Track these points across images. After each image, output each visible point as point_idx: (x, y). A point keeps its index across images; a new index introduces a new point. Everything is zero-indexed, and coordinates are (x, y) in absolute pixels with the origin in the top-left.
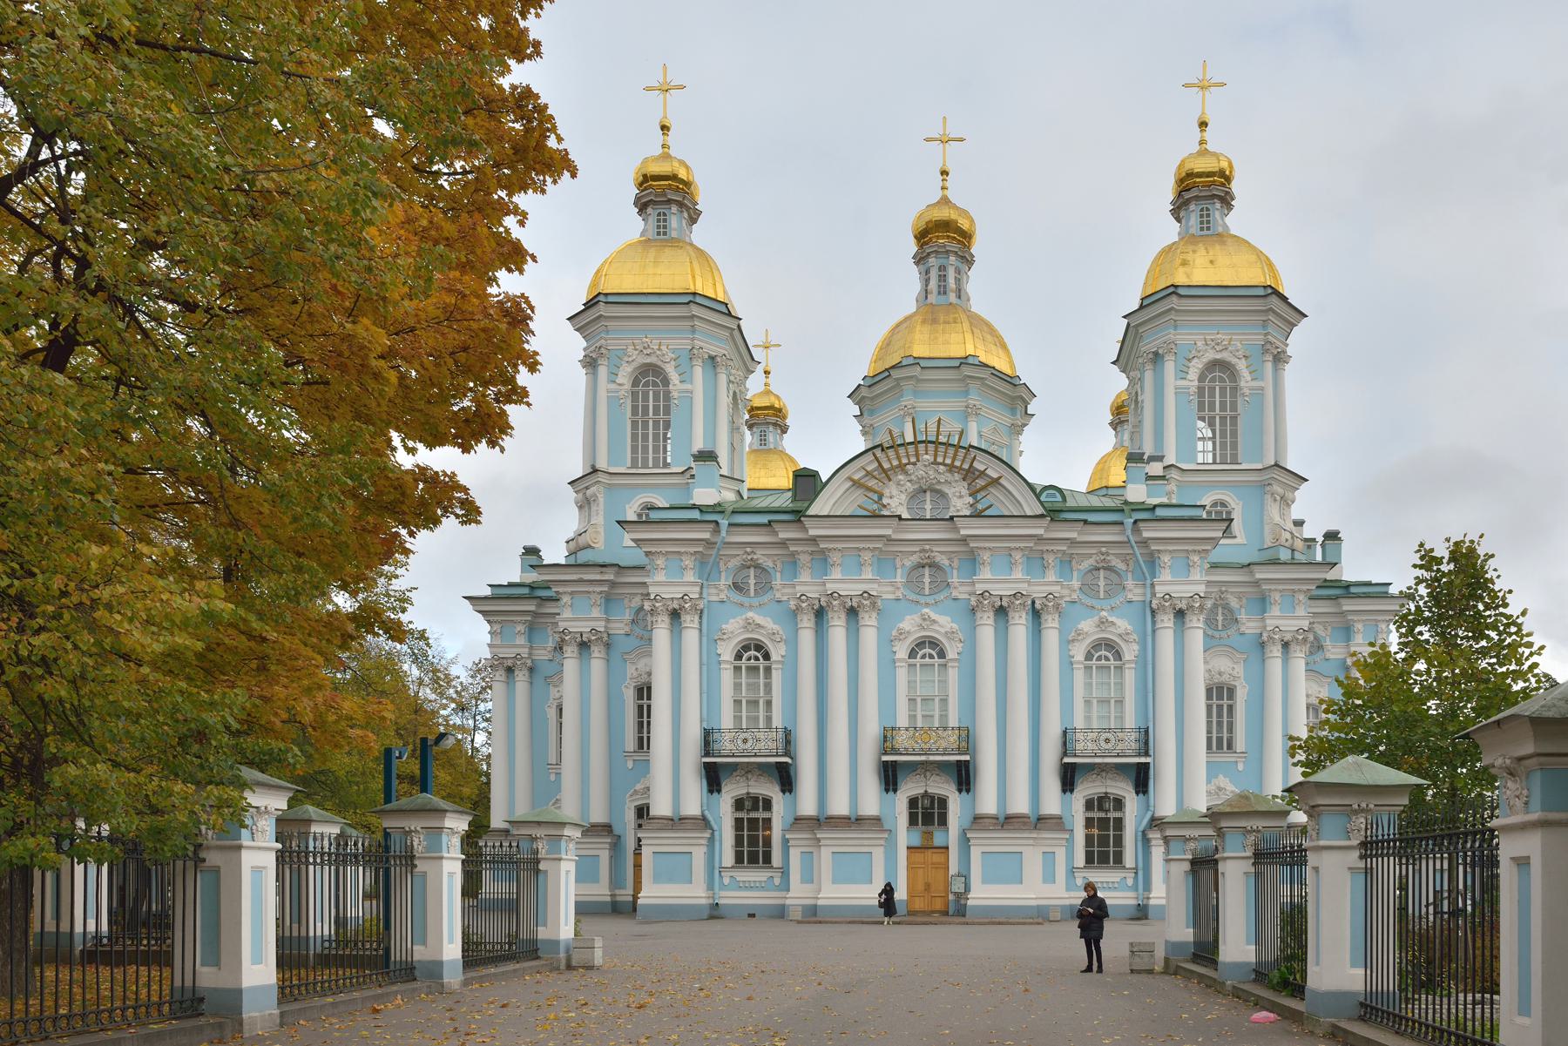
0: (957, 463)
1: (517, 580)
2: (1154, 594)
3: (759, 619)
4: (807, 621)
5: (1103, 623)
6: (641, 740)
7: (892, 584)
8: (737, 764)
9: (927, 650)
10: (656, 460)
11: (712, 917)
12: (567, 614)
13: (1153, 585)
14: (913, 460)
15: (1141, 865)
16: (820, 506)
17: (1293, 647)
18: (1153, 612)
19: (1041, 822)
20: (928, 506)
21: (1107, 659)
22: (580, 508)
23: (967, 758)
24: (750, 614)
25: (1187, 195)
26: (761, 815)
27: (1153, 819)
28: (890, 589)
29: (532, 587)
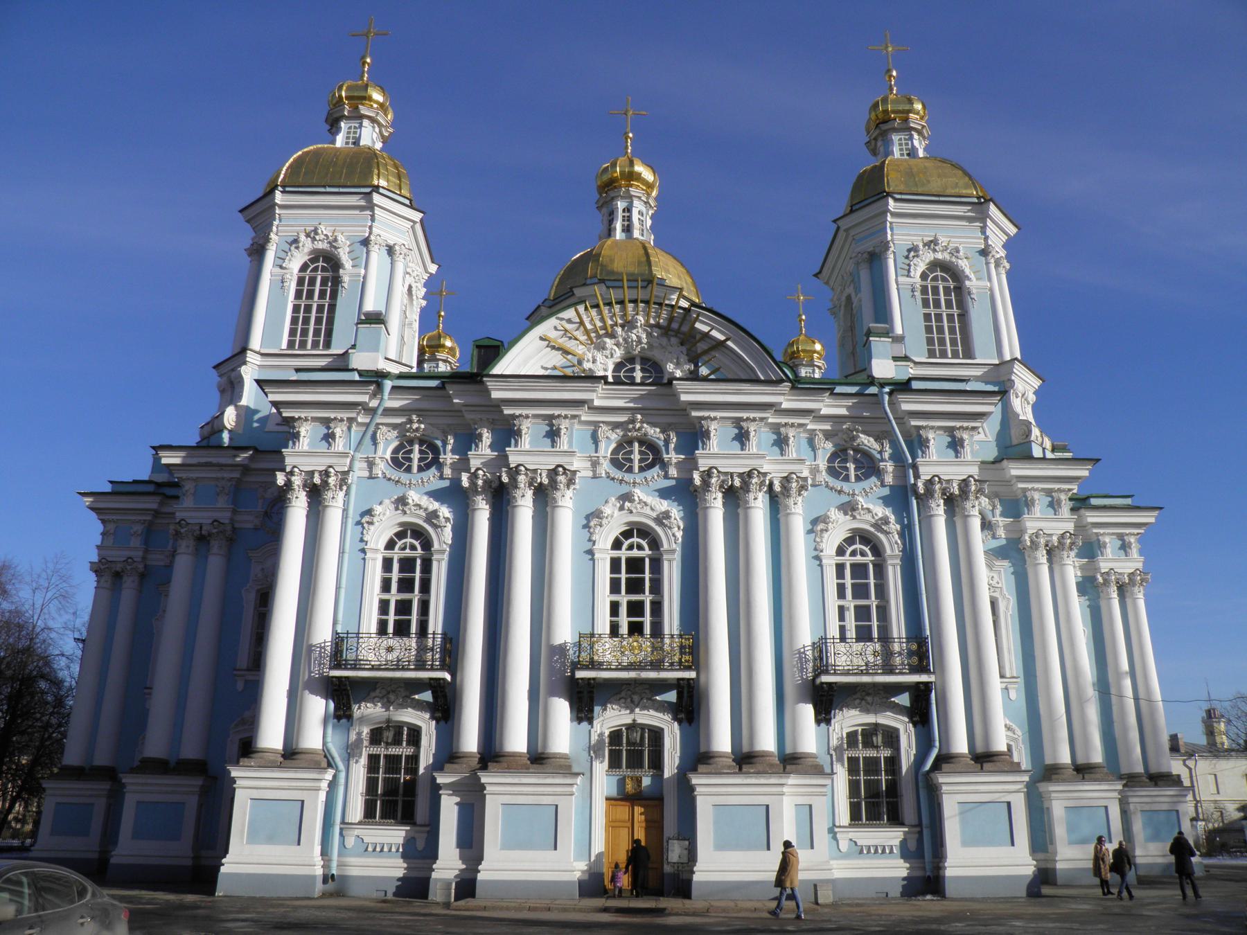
1: (146, 478)
9: (635, 540)
10: (315, 345)
12: (188, 502)
13: (915, 467)
15: (925, 821)
22: (222, 391)
23: (693, 675)
25: (884, 127)
29: (159, 485)
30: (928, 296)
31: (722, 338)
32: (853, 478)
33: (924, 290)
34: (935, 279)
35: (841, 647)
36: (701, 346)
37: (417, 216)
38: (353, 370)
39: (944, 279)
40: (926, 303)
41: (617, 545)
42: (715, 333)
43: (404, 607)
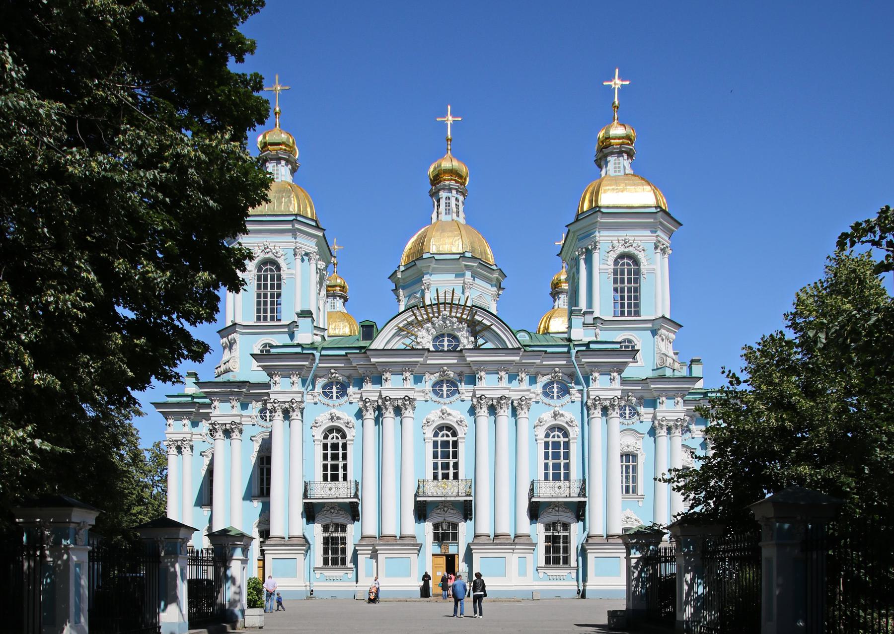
0: (464, 317)
2: (588, 397)
3: (338, 413)
5: (555, 415)
6: (262, 489)
8: (324, 503)
11: (308, 598)
14: (436, 315)
16: (378, 343)
17: (673, 431)
18: (588, 409)
19: (518, 541)
20: (446, 343)
21: (558, 437)
24: (333, 411)
26: (339, 535)
27: (589, 537)
30: (617, 276)
31: (488, 324)
32: (555, 397)
33: (615, 272)
34: (623, 264)
35: (543, 484)
37: (321, 234)
38: (299, 345)
39: (629, 265)
40: (615, 281)
41: (436, 435)
43: (335, 468)
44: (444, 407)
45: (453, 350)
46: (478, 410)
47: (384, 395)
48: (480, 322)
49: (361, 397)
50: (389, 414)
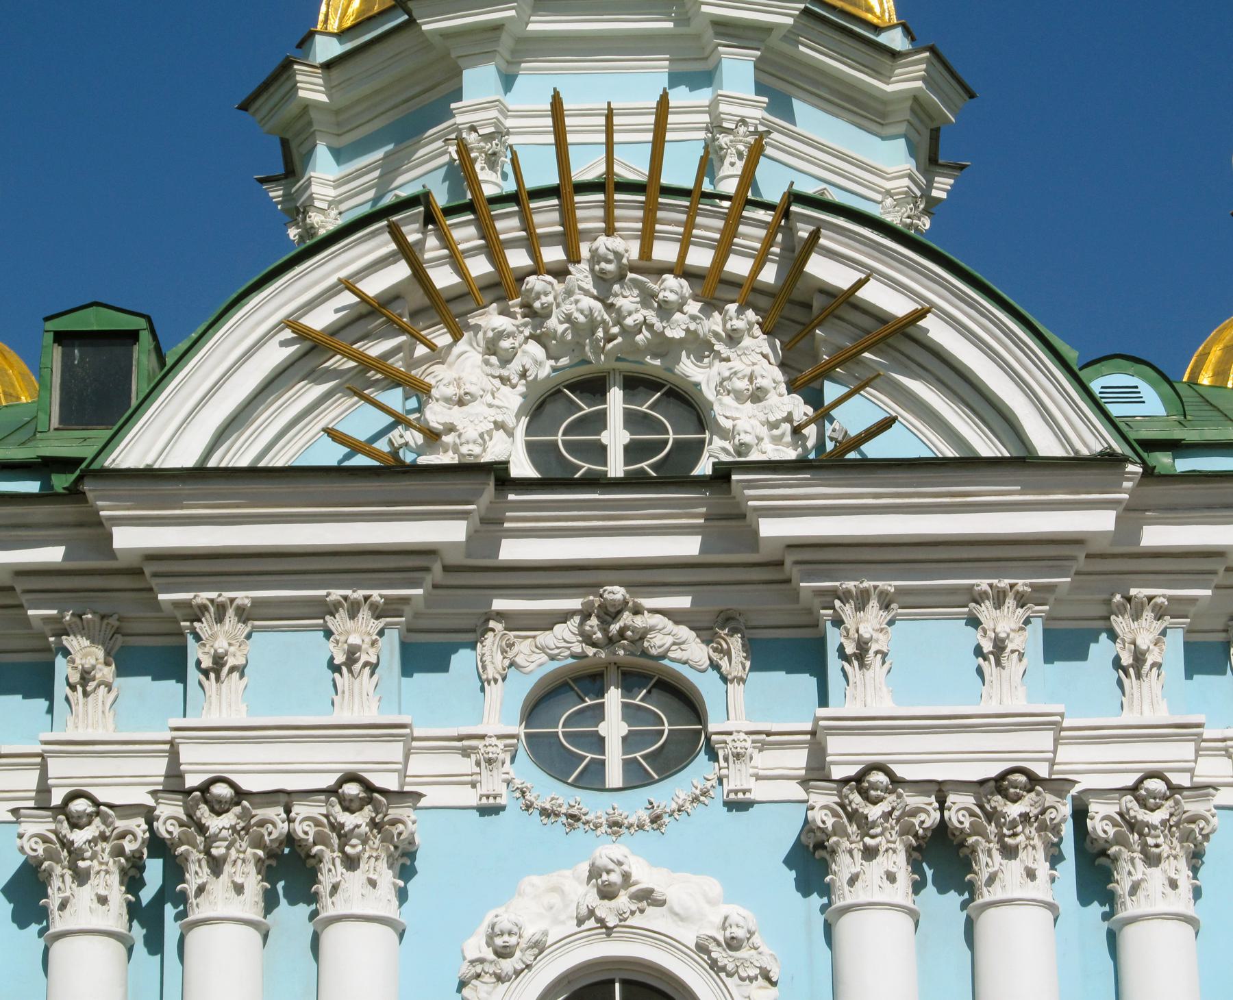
4: (91, 904)
7: (465, 744)
28: (465, 766)
36: (827, 339)
42: (874, 294)
44: (608, 850)
45: (666, 473)
46: (844, 866)
47: (199, 761)
48: (843, 302)
49: (44, 790)
50: (228, 897)
